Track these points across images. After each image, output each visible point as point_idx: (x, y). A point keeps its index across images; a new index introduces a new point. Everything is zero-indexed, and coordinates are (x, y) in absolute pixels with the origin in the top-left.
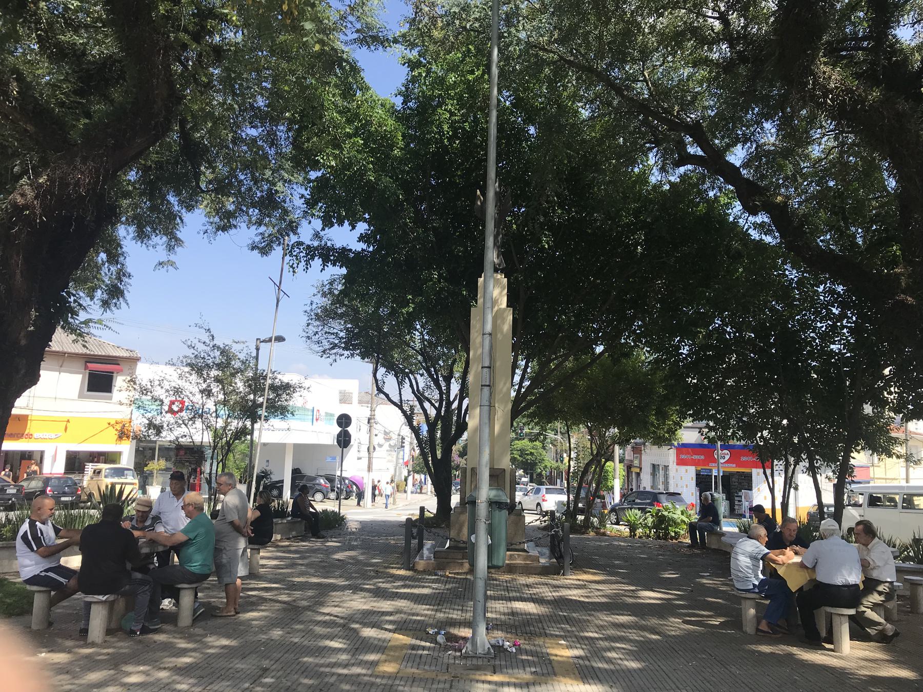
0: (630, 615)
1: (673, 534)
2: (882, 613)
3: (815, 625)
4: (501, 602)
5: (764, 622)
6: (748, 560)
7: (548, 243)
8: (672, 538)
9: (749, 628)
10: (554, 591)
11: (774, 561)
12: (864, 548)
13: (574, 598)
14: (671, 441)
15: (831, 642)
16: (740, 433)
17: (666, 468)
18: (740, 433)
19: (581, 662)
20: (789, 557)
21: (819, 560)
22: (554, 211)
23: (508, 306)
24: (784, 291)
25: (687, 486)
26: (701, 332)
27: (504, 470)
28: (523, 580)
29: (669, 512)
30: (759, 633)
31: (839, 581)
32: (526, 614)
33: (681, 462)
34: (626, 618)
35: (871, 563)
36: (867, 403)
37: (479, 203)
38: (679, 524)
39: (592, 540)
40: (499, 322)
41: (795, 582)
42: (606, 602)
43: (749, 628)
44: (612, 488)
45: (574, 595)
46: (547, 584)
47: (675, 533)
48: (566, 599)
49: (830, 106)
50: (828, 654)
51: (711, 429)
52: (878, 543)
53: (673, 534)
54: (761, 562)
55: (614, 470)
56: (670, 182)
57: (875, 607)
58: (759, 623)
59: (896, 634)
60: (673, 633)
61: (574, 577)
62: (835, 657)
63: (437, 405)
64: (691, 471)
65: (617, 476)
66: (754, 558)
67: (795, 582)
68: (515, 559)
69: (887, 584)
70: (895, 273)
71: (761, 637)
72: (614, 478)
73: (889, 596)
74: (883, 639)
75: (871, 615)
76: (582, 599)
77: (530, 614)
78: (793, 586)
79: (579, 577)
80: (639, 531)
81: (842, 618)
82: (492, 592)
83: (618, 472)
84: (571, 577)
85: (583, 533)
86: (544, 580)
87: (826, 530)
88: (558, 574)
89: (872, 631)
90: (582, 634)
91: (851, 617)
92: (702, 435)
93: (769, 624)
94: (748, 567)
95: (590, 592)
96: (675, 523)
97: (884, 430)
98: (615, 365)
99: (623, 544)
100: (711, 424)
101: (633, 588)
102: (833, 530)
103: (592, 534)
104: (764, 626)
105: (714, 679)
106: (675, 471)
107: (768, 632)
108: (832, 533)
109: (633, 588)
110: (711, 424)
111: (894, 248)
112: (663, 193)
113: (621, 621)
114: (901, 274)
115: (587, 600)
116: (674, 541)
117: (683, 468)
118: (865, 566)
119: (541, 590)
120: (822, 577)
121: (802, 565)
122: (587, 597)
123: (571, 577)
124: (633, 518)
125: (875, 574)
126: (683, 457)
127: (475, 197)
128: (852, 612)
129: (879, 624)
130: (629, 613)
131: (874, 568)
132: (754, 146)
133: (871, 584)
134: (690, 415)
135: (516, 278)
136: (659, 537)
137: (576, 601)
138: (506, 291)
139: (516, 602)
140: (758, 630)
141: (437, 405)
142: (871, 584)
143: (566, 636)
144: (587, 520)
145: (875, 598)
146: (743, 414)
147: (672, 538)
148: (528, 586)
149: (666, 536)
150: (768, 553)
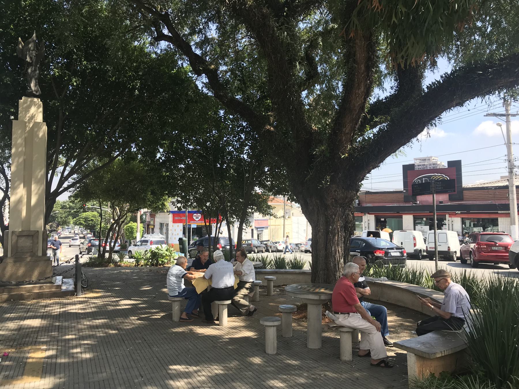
0: (106, 319)
1: (160, 262)
2: (248, 299)
3: (211, 311)
4: (16, 321)
5: (184, 313)
6: (175, 279)
7: (76, 82)
8: (160, 265)
9: (176, 318)
10: (63, 308)
11: (191, 278)
12: (240, 264)
13: (74, 311)
14: (162, 209)
15: (218, 319)
16: (195, 204)
17: (167, 225)
18: (195, 204)
19: (49, 360)
20: (198, 275)
21: (213, 275)
22: (81, 61)
23: (43, 121)
24: (218, 123)
25: (178, 234)
26: (166, 144)
27: (38, 231)
28: (44, 302)
29: (159, 250)
30: (181, 320)
31: (222, 285)
32: (30, 328)
33: (174, 221)
34: (100, 321)
35: (243, 272)
36: (256, 186)
37: (20, 46)
38: (164, 257)
39: (111, 270)
40: (36, 129)
41: (200, 289)
42: (92, 312)
43: (176, 318)
44: (136, 237)
45: (76, 309)
46: (60, 303)
47: (162, 261)
48: (68, 313)
49: (227, 4)
50: (215, 328)
51: (178, 202)
52: (247, 261)
53: (160, 262)
54: (183, 280)
55: (137, 227)
56: (156, 53)
57: (245, 297)
58: (181, 314)
59: (255, 310)
60: (128, 327)
61: (84, 296)
62: (218, 329)
63: (5, 189)
64: (181, 226)
65: (139, 231)
66: (178, 277)
67: (200, 289)
68: (44, 289)
69: (250, 283)
70: (268, 115)
71: (182, 322)
72: (137, 232)
73: (251, 289)
74: (249, 314)
75: (243, 302)
76: (80, 311)
77: (33, 328)
78: (199, 290)
79: (87, 296)
80: (142, 262)
81: (224, 306)
82: (15, 314)
83: (139, 229)
84: (81, 296)
85: (107, 266)
86: (57, 300)
87: (216, 257)
88: (74, 295)
89: (243, 311)
90: (64, 338)
91: (228, 305)
92: (174, 205)
93: (187, 315)
94: (175, 283)
95: (88, 305)
96: (163, 257)
97: (265, 201)
98: (125, 165)
99: (127, 271)
100: (180, 199)
101: (119, 299)
102: (220, 256)
103: (112, 265)
104: (184, 316)
105: (138, 358)
106: (172, 226)
107: (186, 319)
108: (219, 258)
109: (119, 299)
110: (180, 199)
111: (268, 101)
112: (152, 60)
113: (97, 323)
114: (271, 116)
115: (83, 311)
116: (162, 266)
117: (176, 224)
118: (238, 274)
119: (51, 308)
120: (214, 285)
121: (204, 277)
122: (84, 309)
123: (81, 296)
124: (138, 255)
125: (245, 279)
126: (176, 218)
127: (18, 43)
128: (229, 302)
129: (245, 306)
130: (104, 317)
131: (244, 275)
132: (204, 36)
133: (241, 284)
134: (167, 194)
135: (54, 104)
136: (152, 265)
137: (76, 313)
138: (41, 109)
139: (28, 320)
140: (181, 318)
141: (5, 189)
142: (241, 284)
143: (50, 341)
144: (110, 256)
145: (244, 291)
146: (196, 193)
147: (160, 265)
148: (46, 306)
149: (157, 264)
150: (186, 273)
